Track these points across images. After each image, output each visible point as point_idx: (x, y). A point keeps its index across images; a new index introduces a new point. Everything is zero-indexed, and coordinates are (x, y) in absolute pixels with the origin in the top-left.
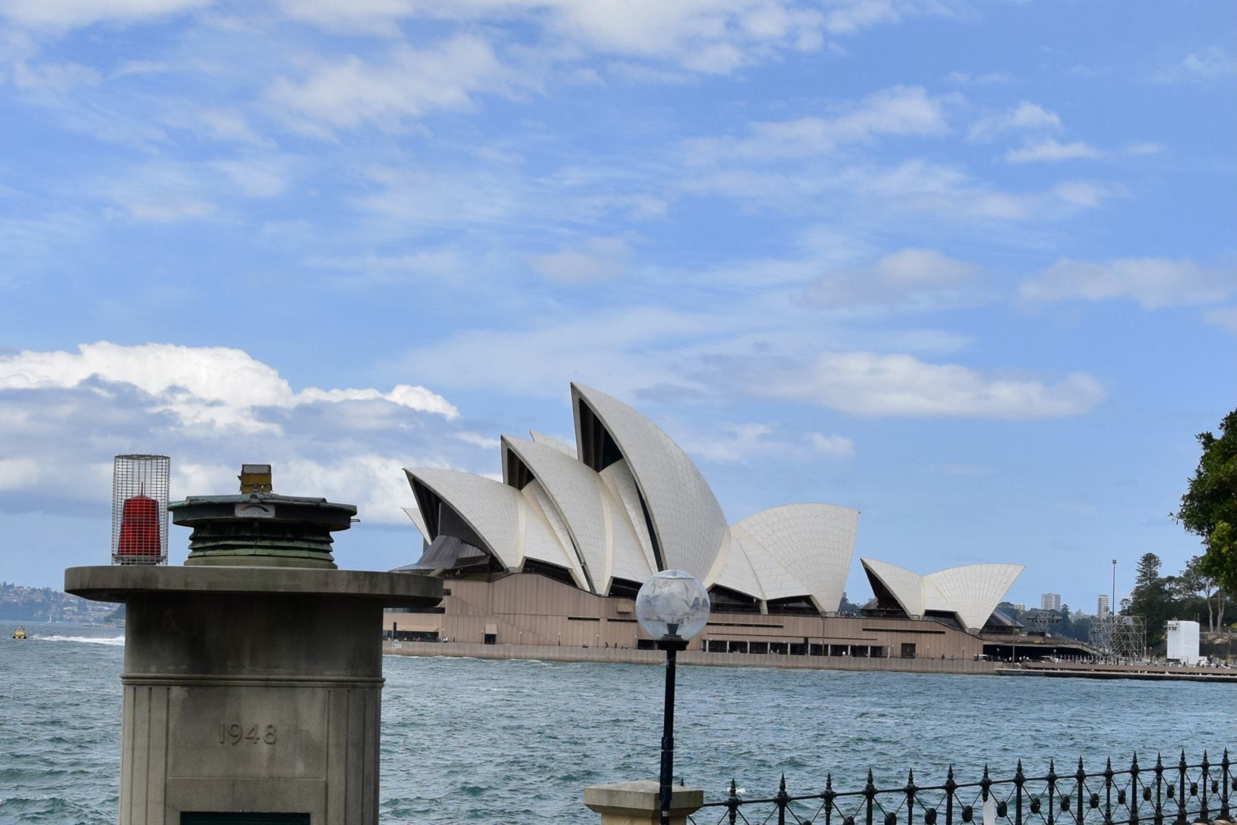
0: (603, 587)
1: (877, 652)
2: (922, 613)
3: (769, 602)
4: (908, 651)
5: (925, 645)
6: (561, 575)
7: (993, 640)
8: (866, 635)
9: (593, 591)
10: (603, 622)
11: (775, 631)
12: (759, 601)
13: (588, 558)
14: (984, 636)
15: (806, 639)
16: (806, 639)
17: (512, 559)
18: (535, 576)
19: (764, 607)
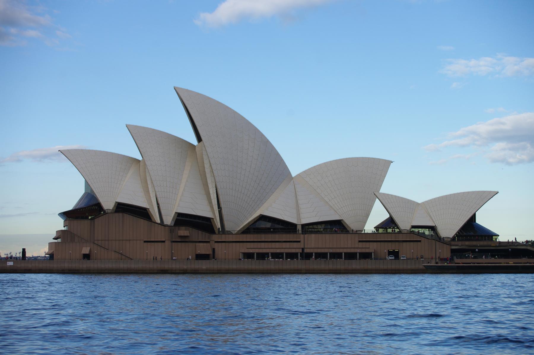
0: (169, 220)
1: (366, 256)
2: (408, 227)
3: (303, 226)
4: (396, 254)
5: (406, 251)
6: (142, 213)
7: (459, 245)
8: (361, 245)
9: (162, 223)
10: (168, 243)
11: (295, 245)
13: (160, 202)
14: (453, 243)
15: (303, 249)
16: (303, 249)
17: (108, 204)
18: (121, 214)
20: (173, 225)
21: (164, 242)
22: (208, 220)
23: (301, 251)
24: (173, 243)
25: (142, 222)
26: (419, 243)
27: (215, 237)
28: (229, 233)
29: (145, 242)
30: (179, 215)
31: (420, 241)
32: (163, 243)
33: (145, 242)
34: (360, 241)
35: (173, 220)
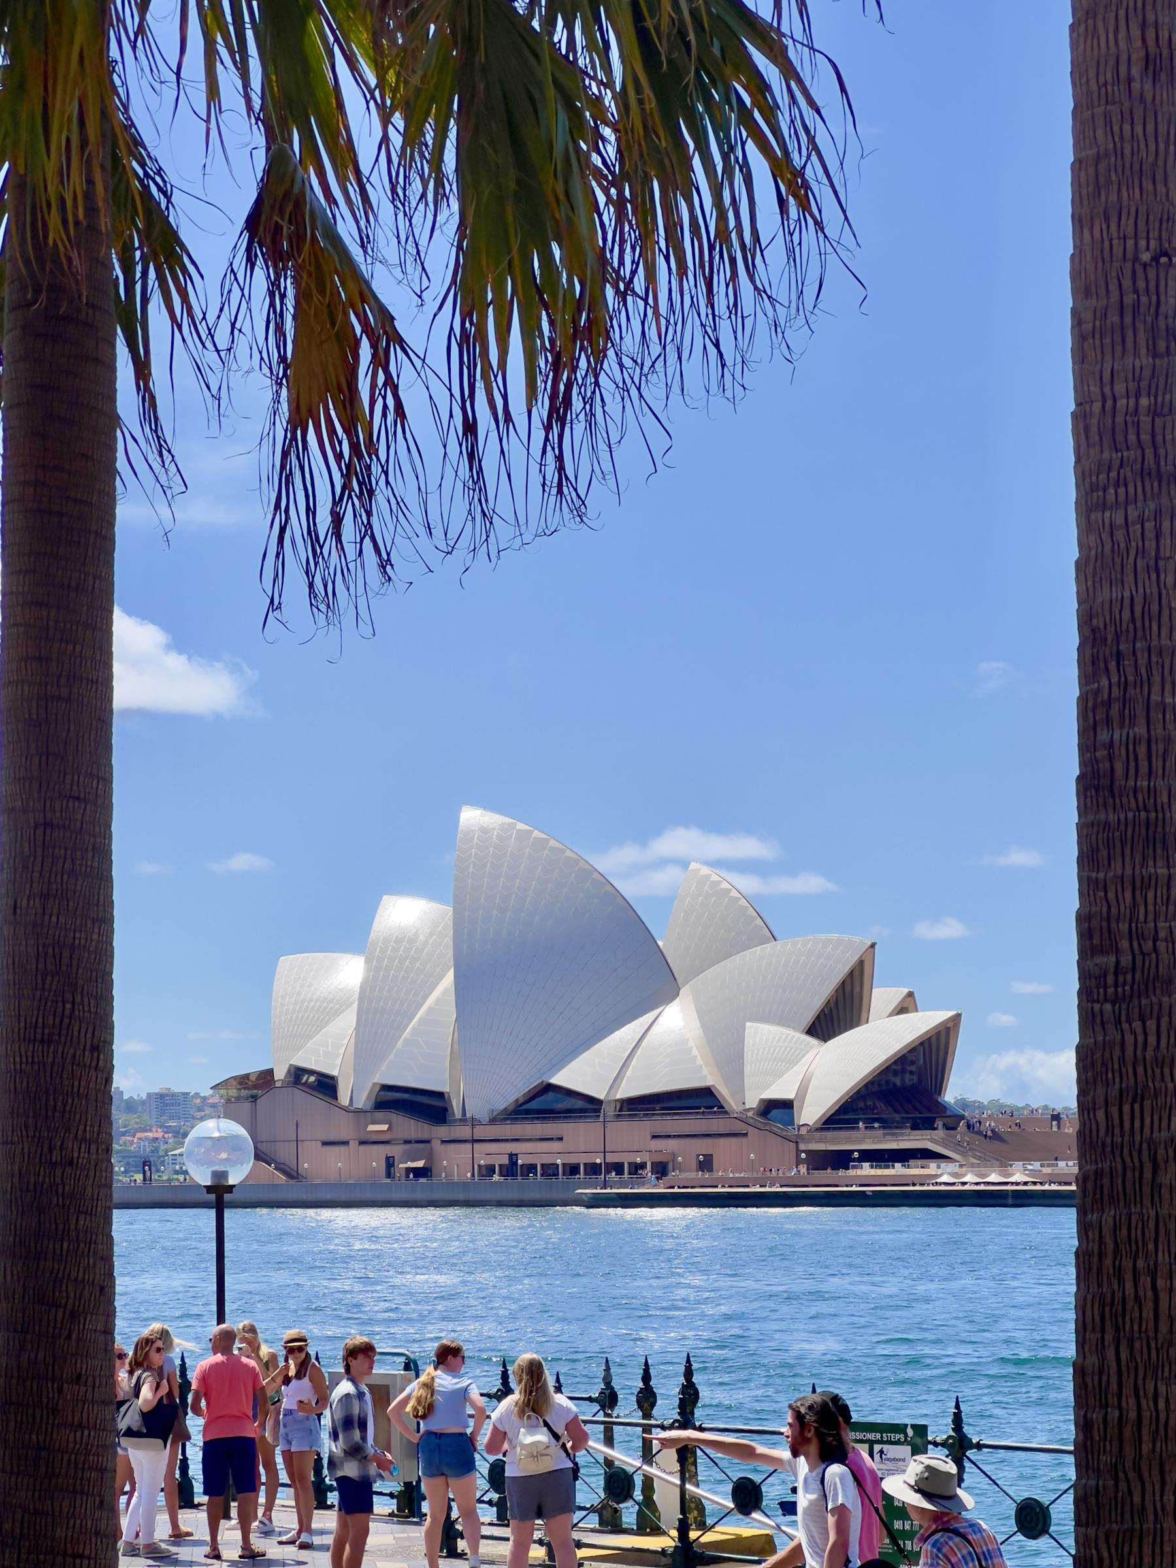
11: (555, 1146)
12: (598, 1102)
15: (513, 1157)
19: (609, 1111)
20: (369, 1106)
21: (346, 1143)
22: (440, 1095)
23: (505, 1160)
24: (362, 1147)
25: (317, 1103)
26: (744, 1140)
27: (442, 1131)
28: (474, 1122)
29: (325, 1144)
30: (386, 1088)
31: (746, 1135)
32: (343, 1148)
33: (325, 1144)
34: (654, 1137)
35: (368, 1098)
